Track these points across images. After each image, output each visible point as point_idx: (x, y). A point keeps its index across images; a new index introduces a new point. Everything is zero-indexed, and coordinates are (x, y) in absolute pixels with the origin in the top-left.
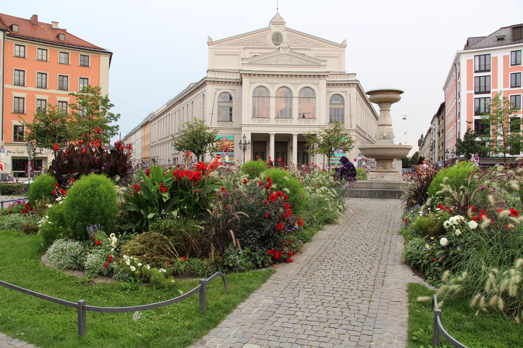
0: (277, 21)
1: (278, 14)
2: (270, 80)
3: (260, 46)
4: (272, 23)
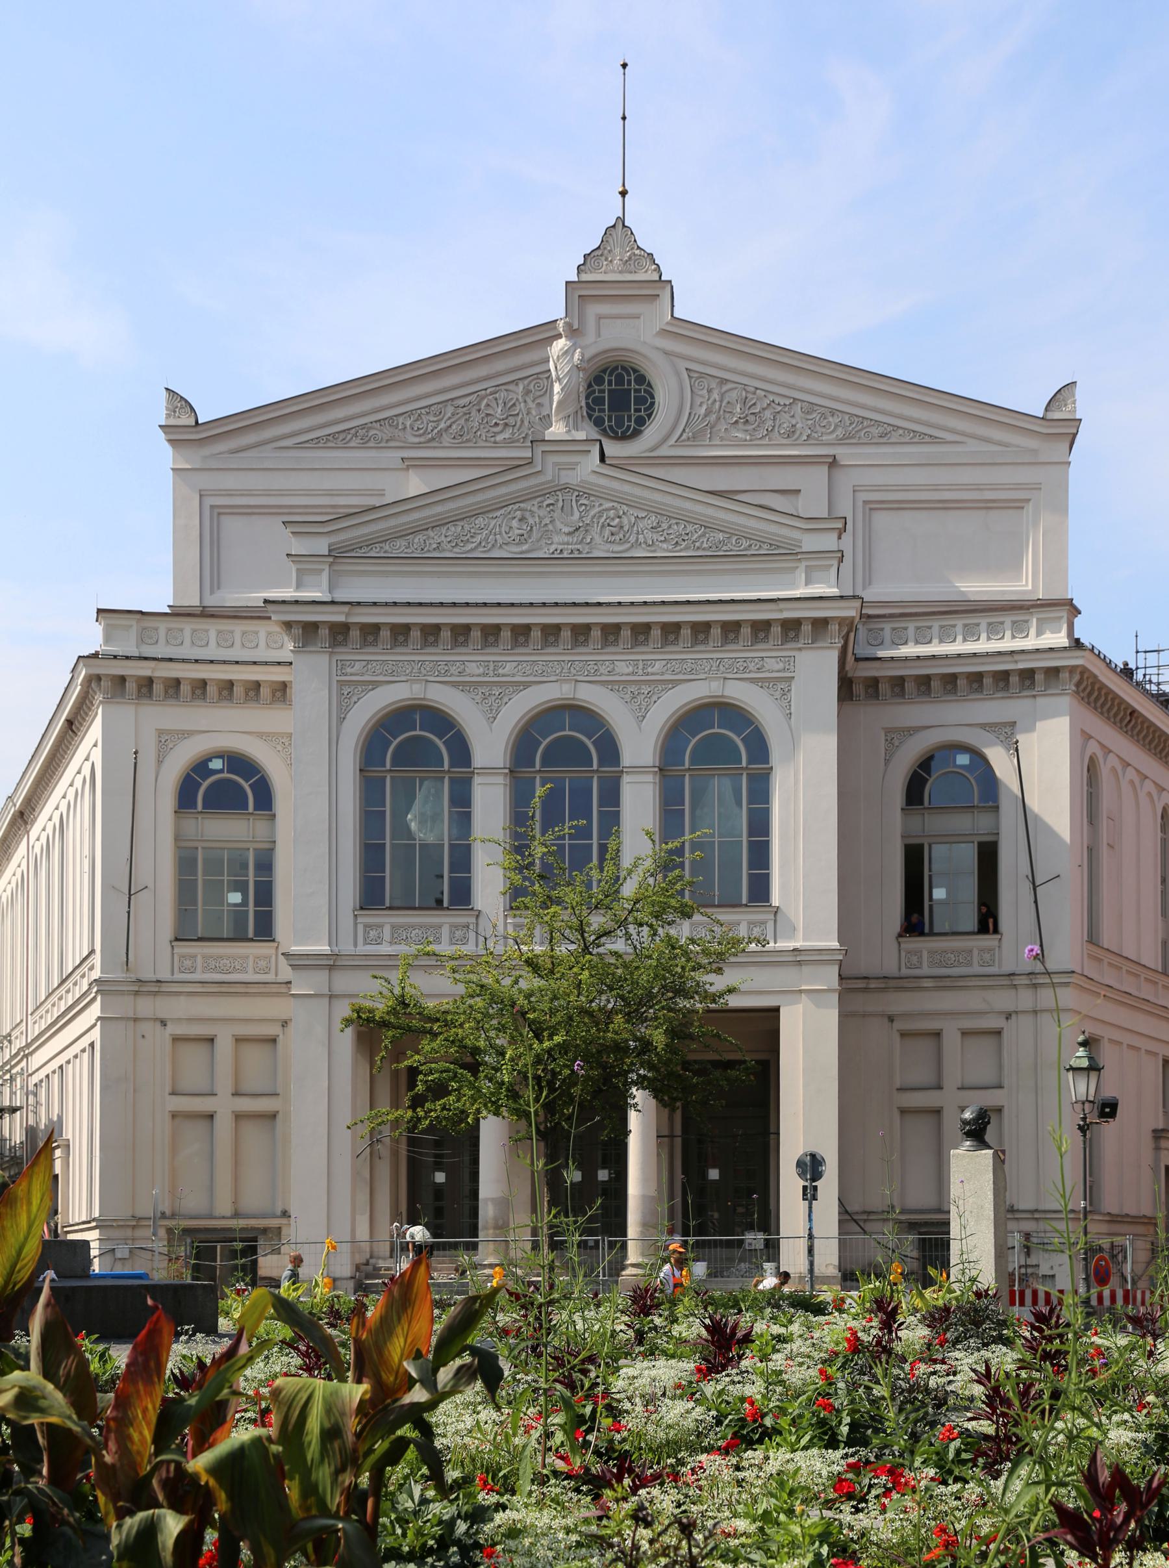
0: (617, 274)
1: (619, 228)
2: (473, 662)
3: (509, 443)
4: (578, 293)
